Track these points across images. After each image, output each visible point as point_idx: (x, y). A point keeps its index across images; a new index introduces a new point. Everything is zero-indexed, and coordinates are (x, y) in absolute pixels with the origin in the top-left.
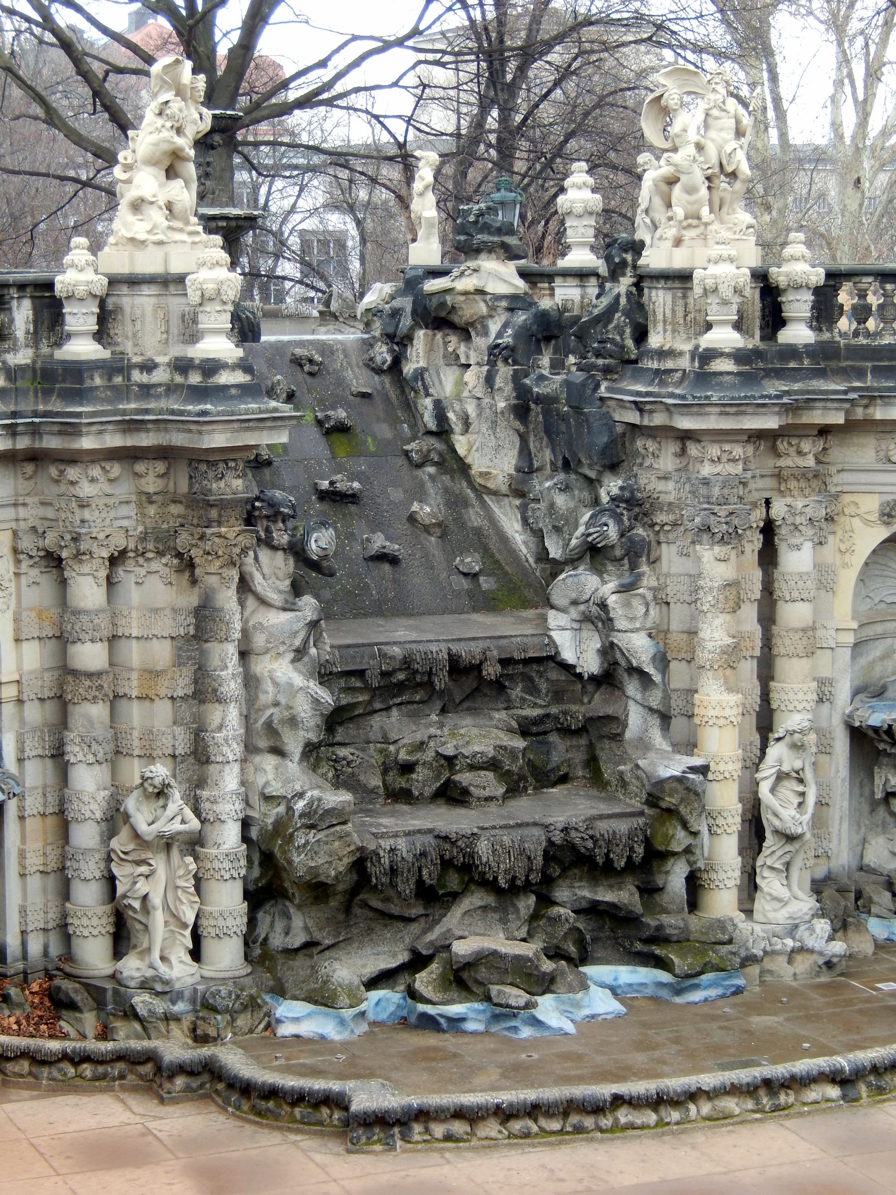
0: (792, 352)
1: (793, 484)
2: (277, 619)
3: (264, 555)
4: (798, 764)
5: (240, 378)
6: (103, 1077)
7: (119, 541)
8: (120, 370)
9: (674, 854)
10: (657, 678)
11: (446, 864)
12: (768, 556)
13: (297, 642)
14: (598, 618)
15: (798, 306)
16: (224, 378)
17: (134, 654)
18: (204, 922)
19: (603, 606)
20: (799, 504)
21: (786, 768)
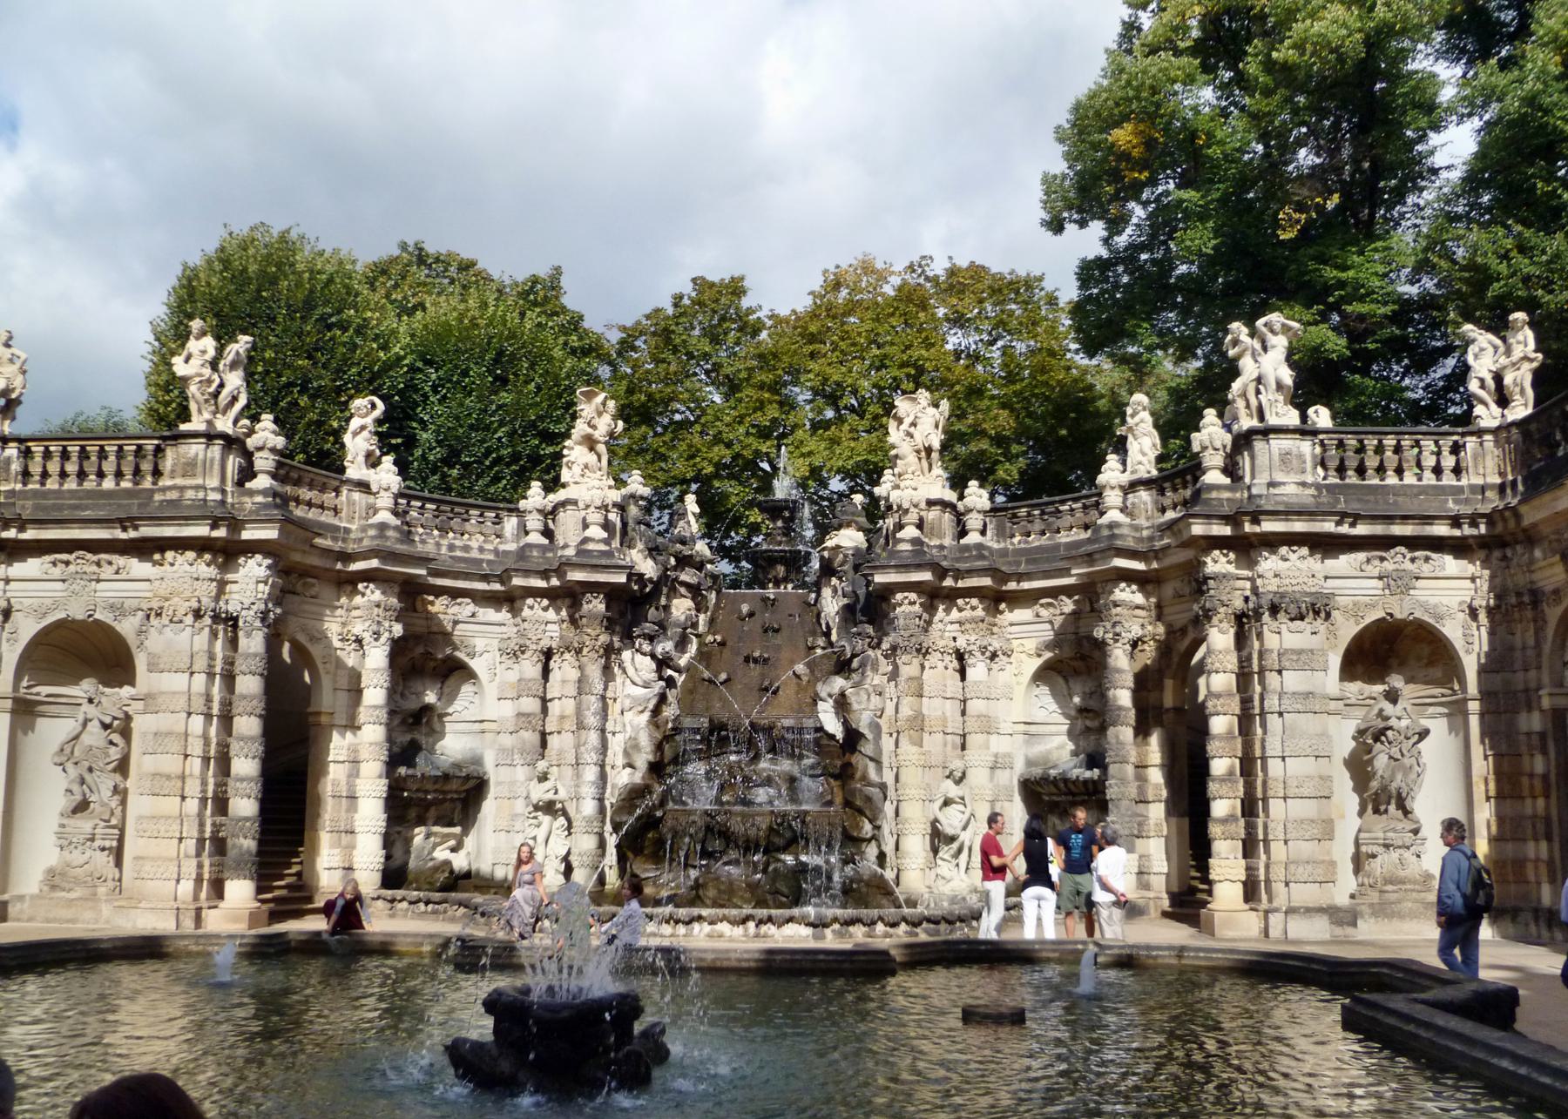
0: (967, 548)
1: (968, 626)
2: (640, 691)
3: (638, 657)
4: (961, 794)
5: (603, 547)
6: (434, 912)
7: (545, 643)
8: (552, 550)
9: (864, 840)
10: (870, 736)
11: (709, 829)
12: (962, 673)
13: (651, 706)
14: (842, 704)
15: (974, 521)
16: (591, 546)
17: (555, 708)
18: (571, 858)
19: (843, 695)
20: (973, 639)
21: (950, 795)
